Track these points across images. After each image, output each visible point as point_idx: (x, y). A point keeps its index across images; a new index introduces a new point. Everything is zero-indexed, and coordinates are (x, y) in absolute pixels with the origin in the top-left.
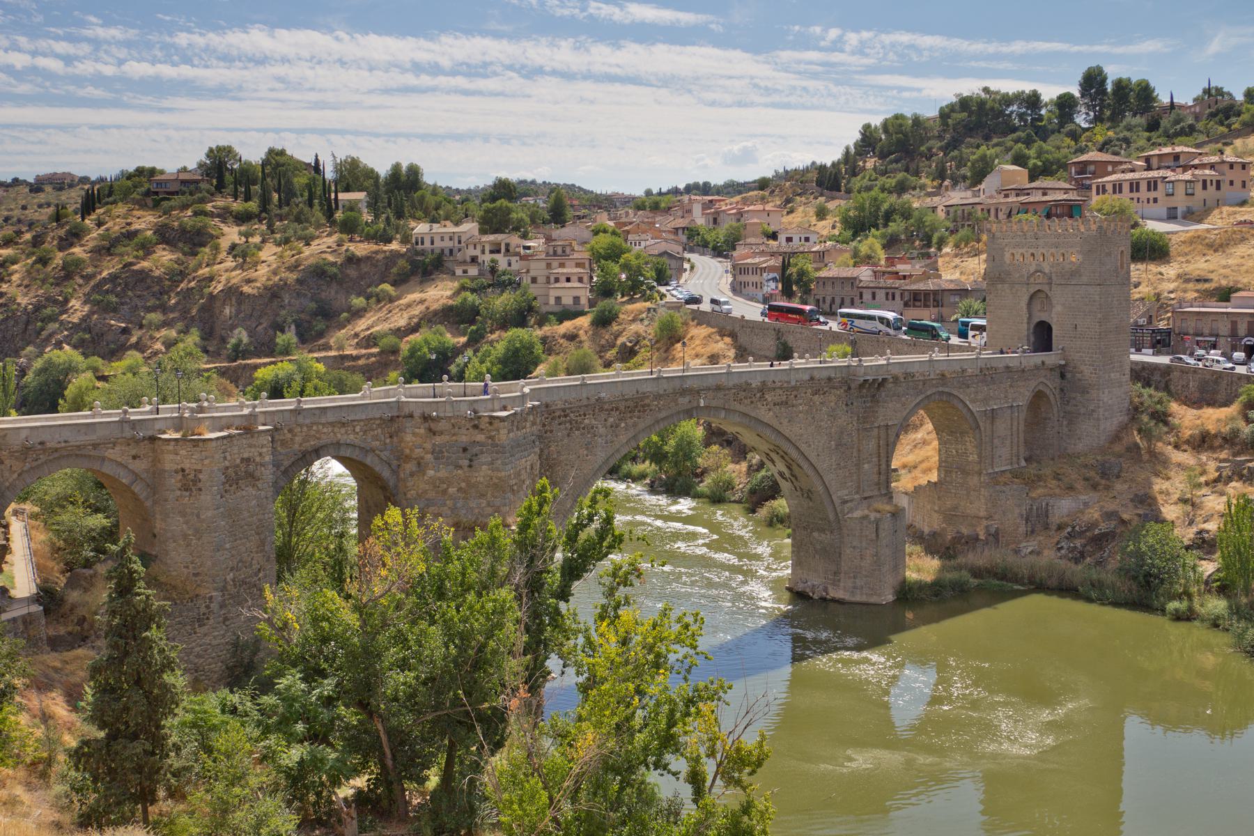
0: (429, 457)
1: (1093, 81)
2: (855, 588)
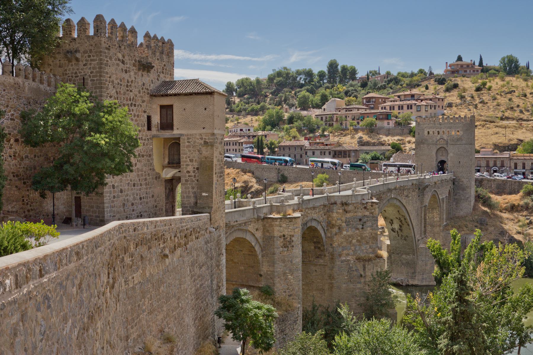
0: (344, 224)
2: (423, 279)
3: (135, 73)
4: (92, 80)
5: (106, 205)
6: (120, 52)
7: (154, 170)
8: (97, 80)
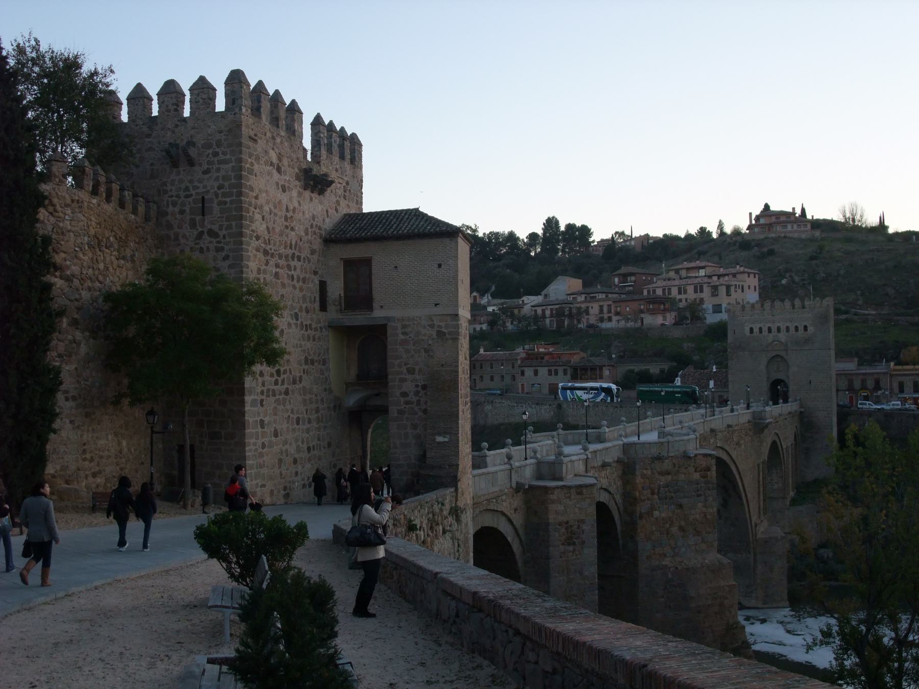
1: (551, 224)
3: (300, 194)
4: (219, 203)
5: (249, 462)
6: (273, 149)
7: (330, 391)
8: (232, 202)
